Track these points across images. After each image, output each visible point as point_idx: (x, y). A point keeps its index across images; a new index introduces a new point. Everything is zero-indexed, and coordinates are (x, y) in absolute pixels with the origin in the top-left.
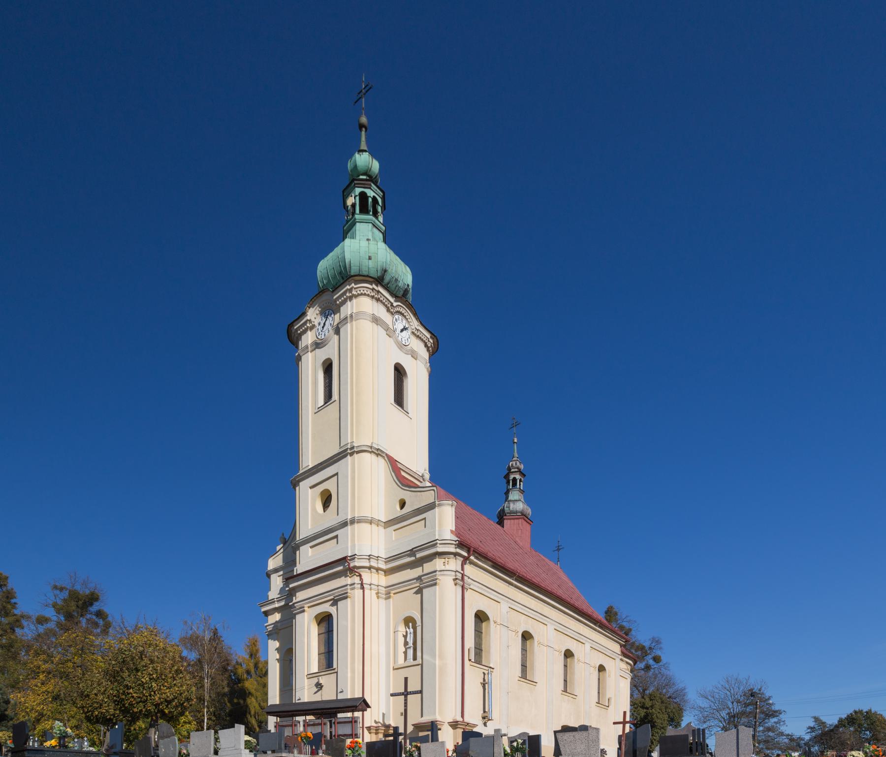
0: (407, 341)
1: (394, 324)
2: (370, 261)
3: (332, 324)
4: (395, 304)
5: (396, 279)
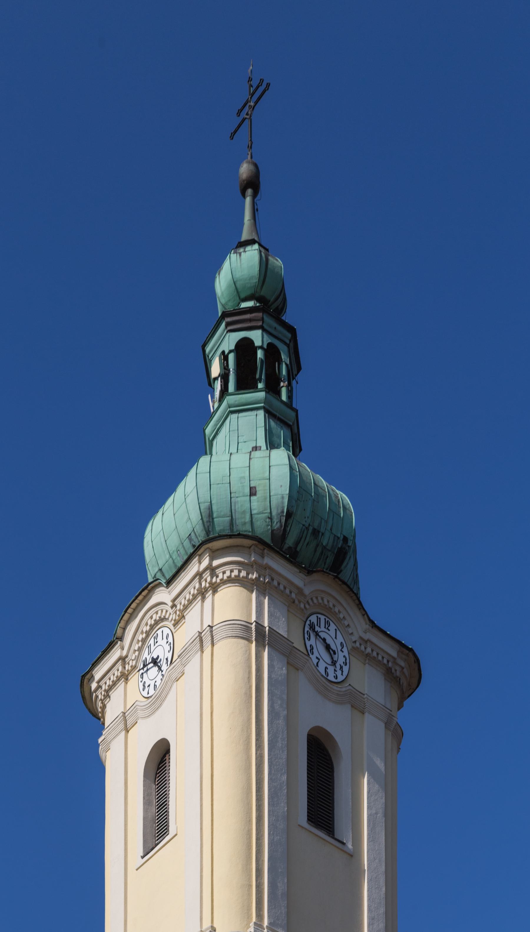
0: (339, 673)
1: (306, 636)
2: (253, 498)
3: (169, 660)
4: (307, 591)
5: (314, 530)
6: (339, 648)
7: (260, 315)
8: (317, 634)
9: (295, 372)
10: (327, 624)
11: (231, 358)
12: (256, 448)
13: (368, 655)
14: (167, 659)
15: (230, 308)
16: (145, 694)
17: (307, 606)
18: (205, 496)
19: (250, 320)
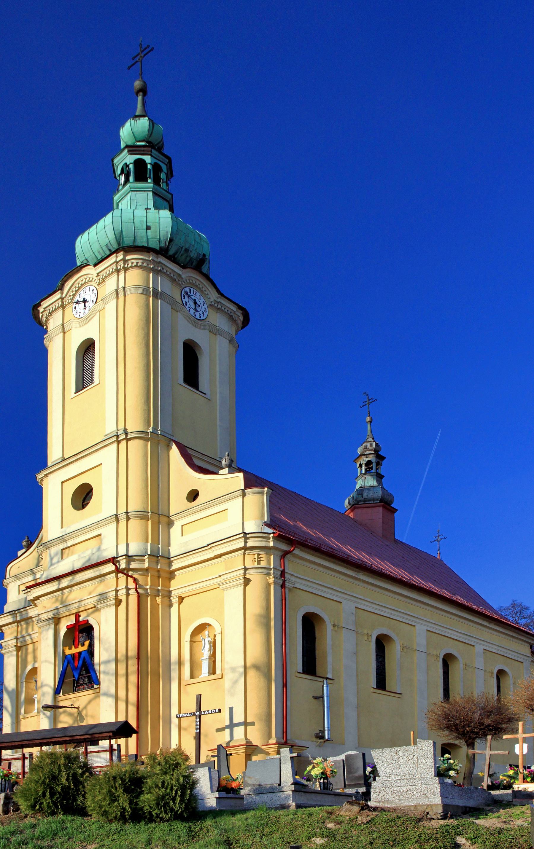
0: (202, 315)
1: (183, 297)
4: (183, 276)
6: (202, 304)
7: (150, 149)
8: (189, 296)
9: (169, 177)
10: (195, 293)
11: (131, 166)
12: (147, 209)
13: (219, 309)
14: (93, 301)
15: (130, 143)
16: (77, 316)
17: (183, 283)
18: (118, 227)
19: (144, 151)
